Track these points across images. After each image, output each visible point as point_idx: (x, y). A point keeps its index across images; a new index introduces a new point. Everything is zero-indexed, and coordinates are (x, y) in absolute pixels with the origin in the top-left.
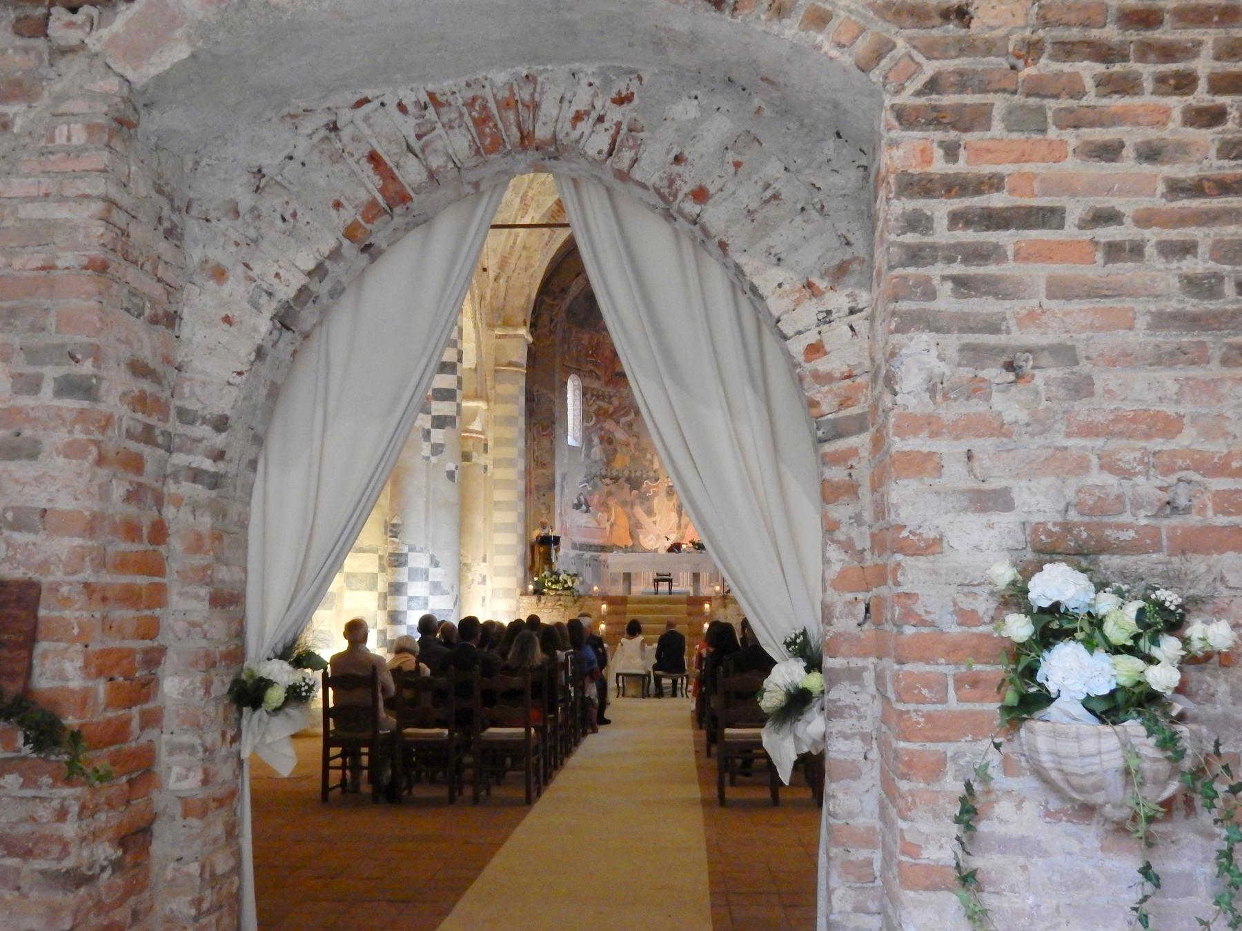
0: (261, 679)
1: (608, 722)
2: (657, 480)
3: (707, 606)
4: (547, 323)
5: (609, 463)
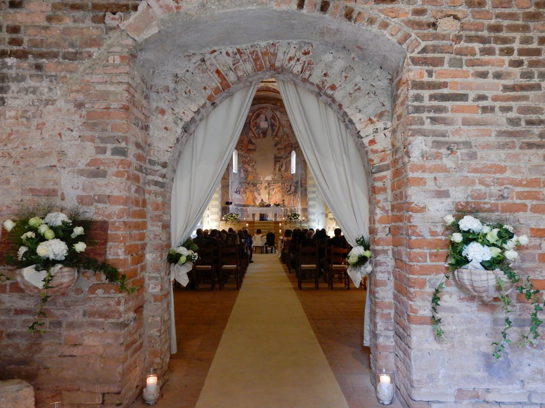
0: (178, 253)
1: (252, 262)
3: (280, 224)
5: (246, 179)
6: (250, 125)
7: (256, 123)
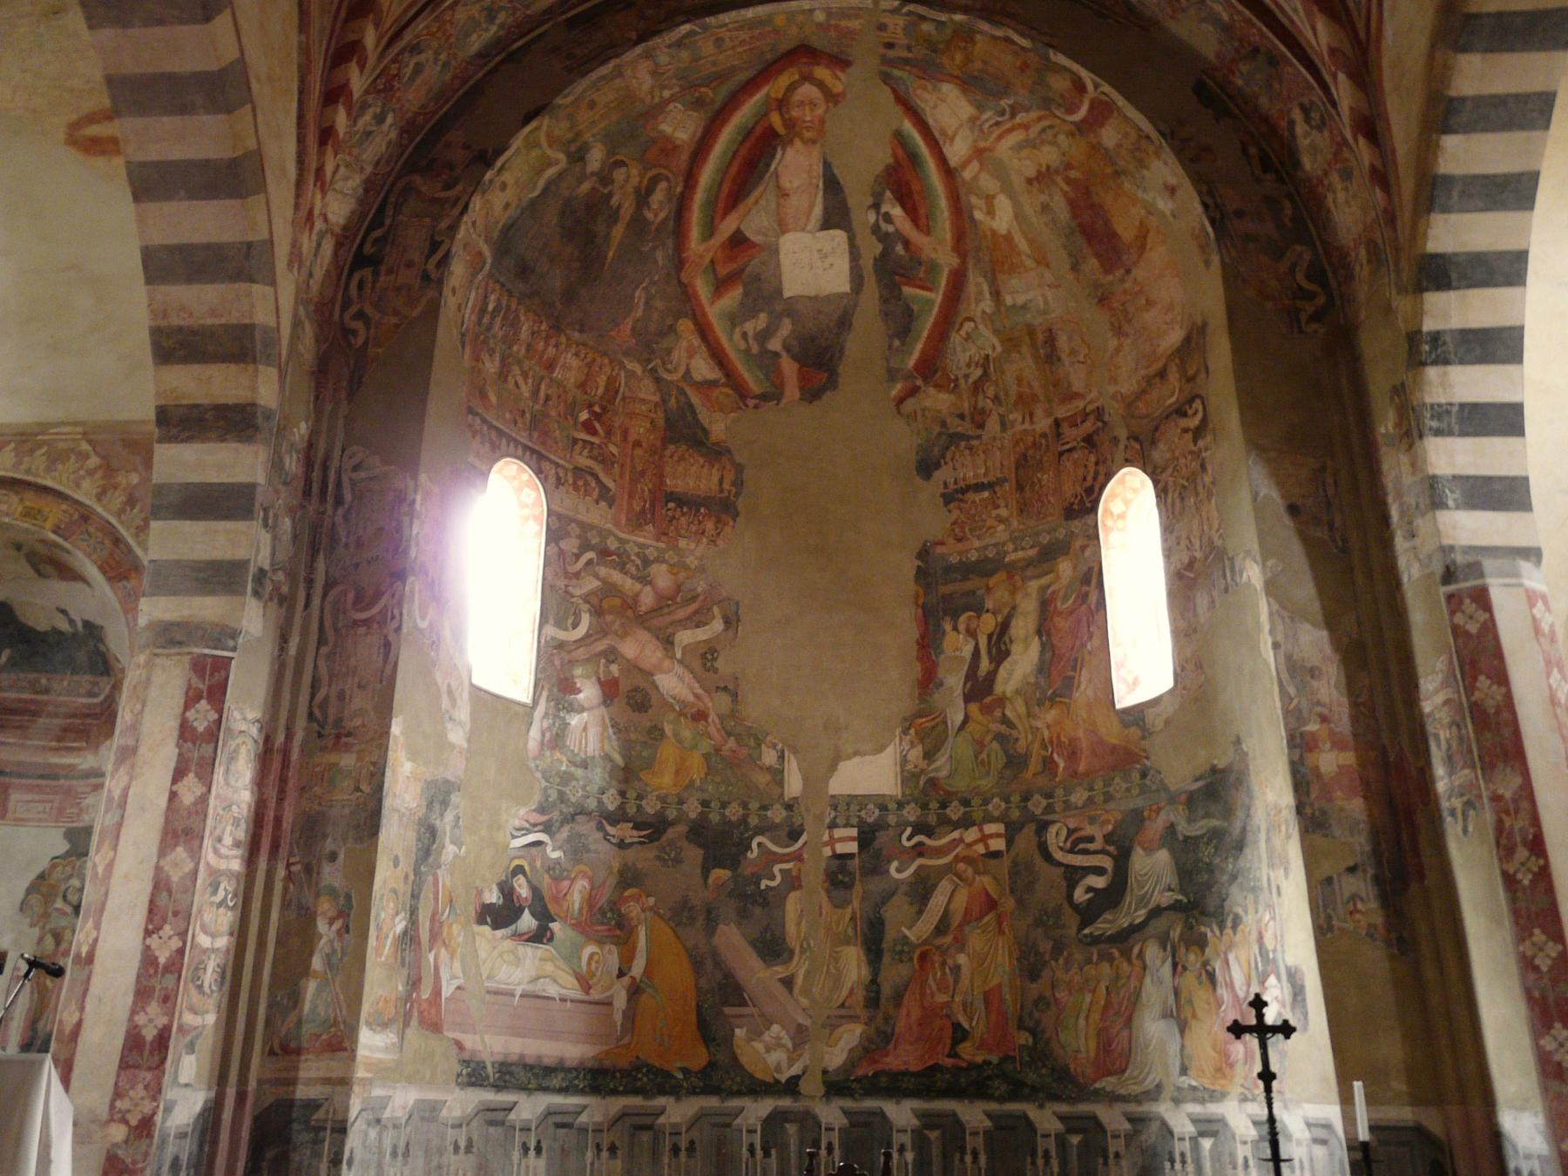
2: (794, 835)
4: (415, 256)
6: (680, 263)
7: (738, 242)
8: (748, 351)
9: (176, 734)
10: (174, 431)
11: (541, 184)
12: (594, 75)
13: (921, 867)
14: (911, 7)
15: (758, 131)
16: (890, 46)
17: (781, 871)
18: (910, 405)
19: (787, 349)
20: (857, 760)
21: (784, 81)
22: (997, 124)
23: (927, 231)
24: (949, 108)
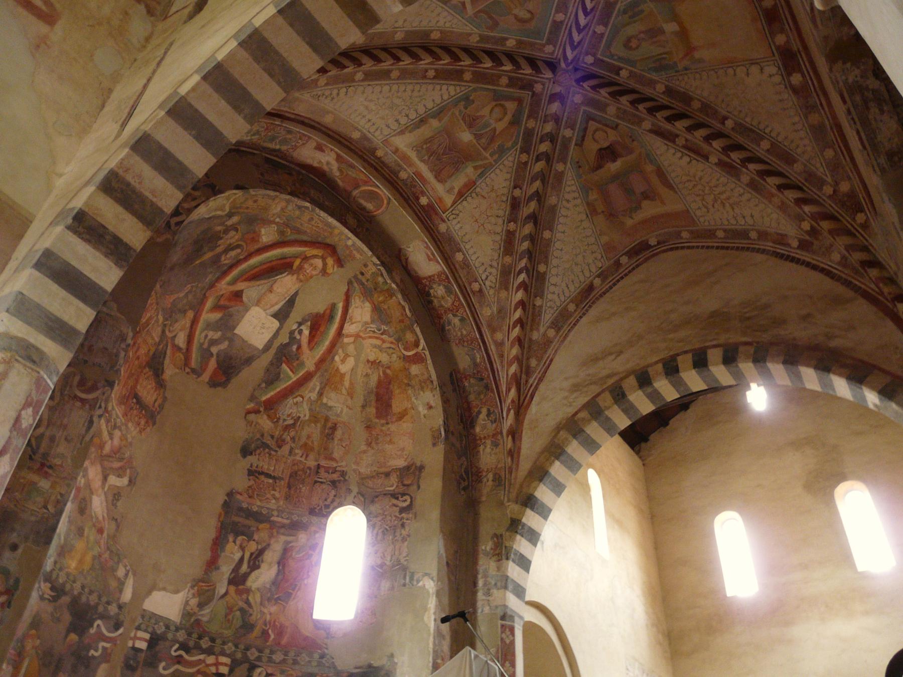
2: (117, 626)
6: (212, 286)
8: (202, 344)
9: (12, 422)
10: (81, 229)
11: (213, 214)
12: (268, 192)
13: (177, 670)
14: (382, 268)
15: (288, 260)
16: (362, 274)
17: (103, 647)
18: (252, 417)
19: (218, 355)
20: (162, 593)
21: (315, 252)
22: (374, 332)
23: (311, 349)
24: (361, 312)
